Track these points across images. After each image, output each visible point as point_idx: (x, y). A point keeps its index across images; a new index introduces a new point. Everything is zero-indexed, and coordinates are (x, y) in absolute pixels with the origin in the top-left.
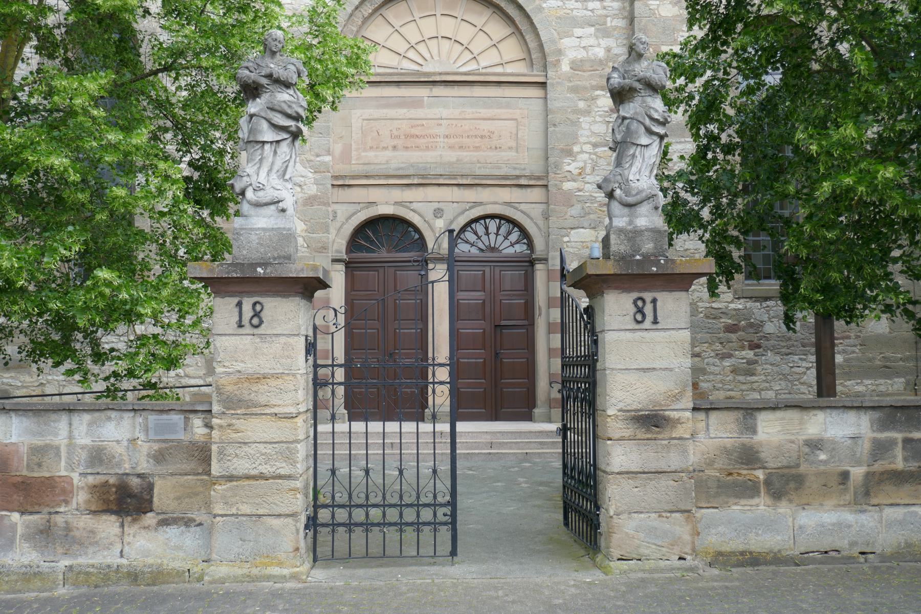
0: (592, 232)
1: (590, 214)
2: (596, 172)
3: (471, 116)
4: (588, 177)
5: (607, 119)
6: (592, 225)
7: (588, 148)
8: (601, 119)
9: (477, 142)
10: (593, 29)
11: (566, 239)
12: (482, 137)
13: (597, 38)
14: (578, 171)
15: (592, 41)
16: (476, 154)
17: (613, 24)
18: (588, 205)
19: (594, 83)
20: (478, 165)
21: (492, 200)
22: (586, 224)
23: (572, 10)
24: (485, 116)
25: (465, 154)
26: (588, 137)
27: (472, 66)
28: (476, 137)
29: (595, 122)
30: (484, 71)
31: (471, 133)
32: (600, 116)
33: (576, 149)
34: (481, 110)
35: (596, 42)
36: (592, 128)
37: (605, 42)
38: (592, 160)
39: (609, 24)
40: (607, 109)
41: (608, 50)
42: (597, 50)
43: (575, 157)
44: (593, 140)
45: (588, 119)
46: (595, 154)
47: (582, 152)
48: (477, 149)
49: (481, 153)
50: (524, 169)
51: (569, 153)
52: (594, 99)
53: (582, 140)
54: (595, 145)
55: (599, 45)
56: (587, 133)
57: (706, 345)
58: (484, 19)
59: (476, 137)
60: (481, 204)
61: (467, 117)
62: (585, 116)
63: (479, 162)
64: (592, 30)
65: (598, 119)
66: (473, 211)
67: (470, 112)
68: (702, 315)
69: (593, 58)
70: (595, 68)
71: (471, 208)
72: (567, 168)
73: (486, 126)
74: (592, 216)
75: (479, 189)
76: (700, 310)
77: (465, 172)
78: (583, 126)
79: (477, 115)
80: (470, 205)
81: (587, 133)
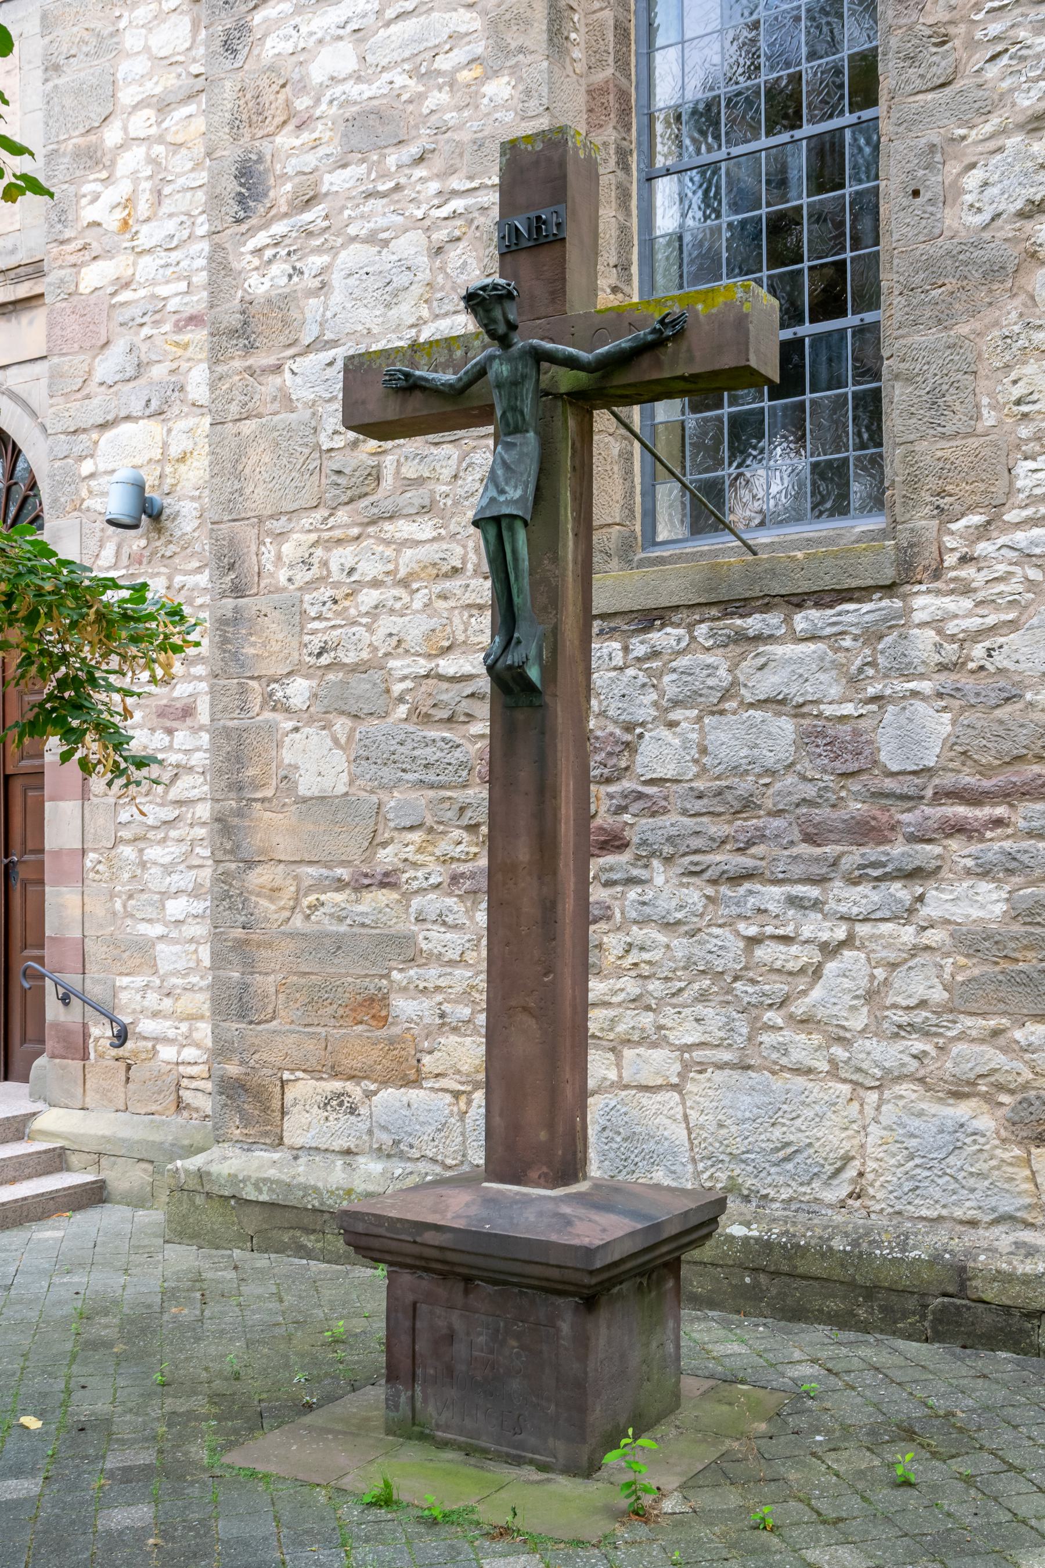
0: (154, 428)
2: (166, 208)
4: (145, 229)
6: (154, 405)
7: (141, 123)
11: (87, 467)
14: (120, 214)
18: (146, 331)
22: (136, 407)
36: (154, 42)
38: (154, 162)
46: (160, 139)
50: (13, 251)
51: (92, 158)
54: (164, 107)
56: (139, 66)
57: (416, 837)
68: (402, 710)
72: (89, 213)
76: (397, 688)
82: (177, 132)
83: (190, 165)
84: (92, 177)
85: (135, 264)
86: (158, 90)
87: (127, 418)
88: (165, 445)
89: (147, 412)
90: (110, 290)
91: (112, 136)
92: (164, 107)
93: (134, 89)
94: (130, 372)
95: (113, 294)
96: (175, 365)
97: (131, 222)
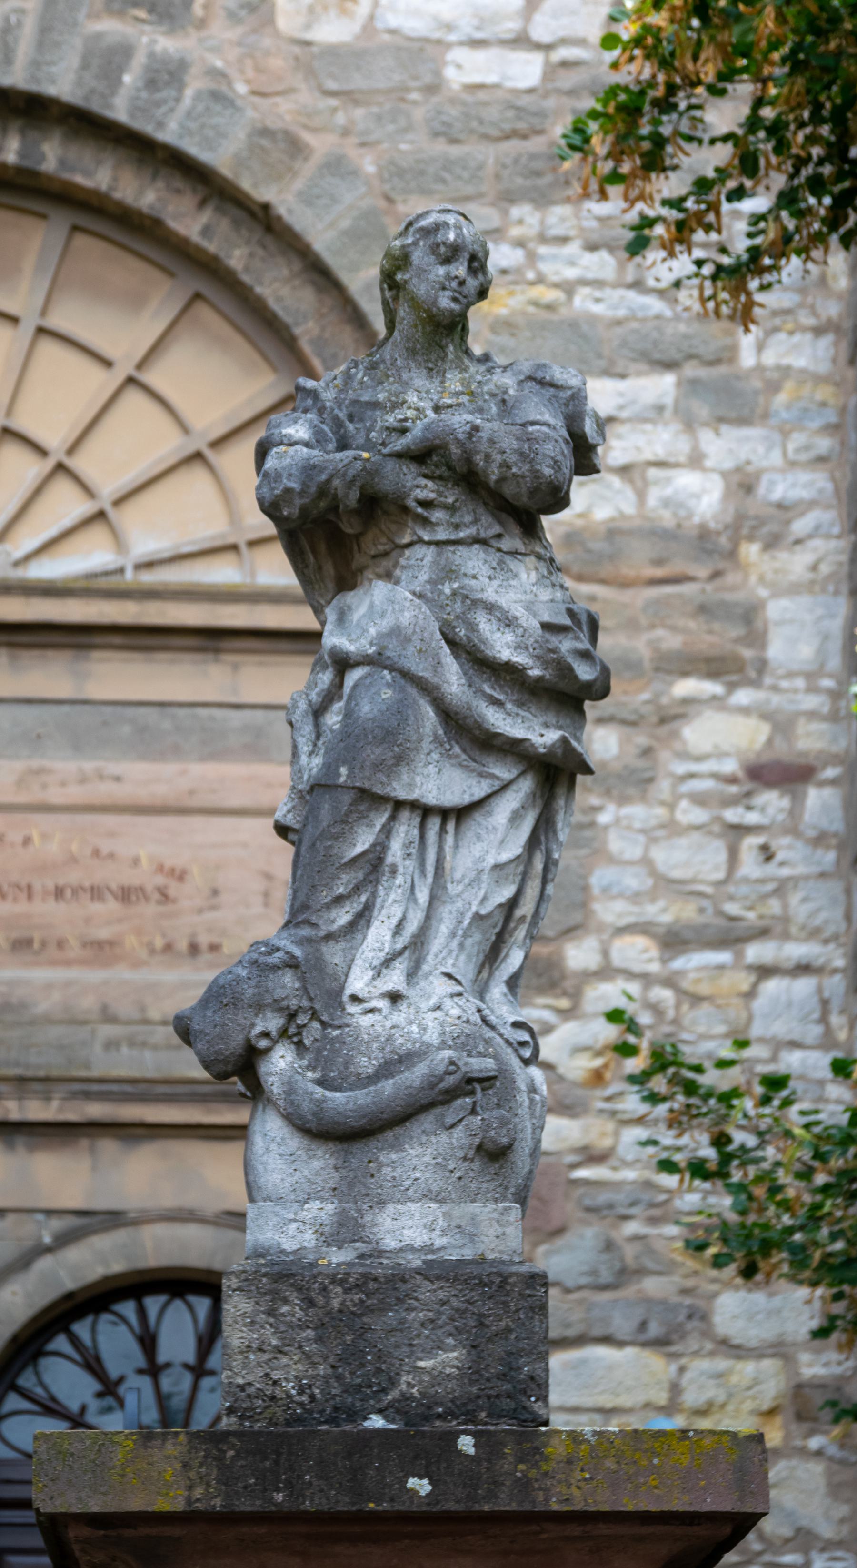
1: (641, 1272)
3: (75, 794)
5: (732, 815)
6: (654, 1330)
7: (636, 952)
8: (699, 815)
9: (104, 918)
10: (668, 381)
12: (126, 895)
13: (689, 425)
15: (662, 440)
16: (95, 976)
17: (770, 358)
18: (632, 1228)
19: (672, 642)
20: (107, 1031)
21: (168, 1199)
23: (569, 288)
24: (143, 795)
25: (40, 974)
26: (636, 897)
27: (89, 557)
28: (96, 893)
29: (672, 828)
30: (148, 578)
31: (73, 877)
32: (700, 800)
33: (579, 955)
34: (113, 768)
35: (683, 447)
36: (660, 856)
37: (724, 447)
39: (747, 359)
40: (730, 766)
41: (743, 483)
42: (686, 481)
43: (576, 996)
44: (664, 913)
45: (637, 813)
46: (669, 982)
47: (606, 971)
48: (101, 951)
49: (122, 973)
52: (670, 717)
53: (609, 912)
54: (673, 941)
55: (696, 461)
58: (149, 327)
59: (96, 893)
60: (114, 1219)
61: (55, 796)
62: (623, 800)
63: (108, 1017)
64: (664, 385)
65: (689, 814)
66: (74, 1254)
67: (67, 773)
69: (667, 519)
70: (676, 567)
71: (64, 1240)
73: (144, 845)
74: (652, 1285)
75: (108, 1146)
77: (41, 1061)
78: (615, 844)
79: (105, 791)
80: (57, 1224)
81: (633, 880)
82: (698, 981)
83: (721, 1029)
84: (541, 1000)
85: (617, 1134)
86: (666, 918)
87: (607, 1340)
88: (675, 1389)
89: (642, 1338)
90: (571, 1159)
91: (579, 955)
92: (673, 941)
93: (619, 906)
94: (606, 1277)
95: (574, 1166)
96: (690, 1283)
97: (608, 1075)
